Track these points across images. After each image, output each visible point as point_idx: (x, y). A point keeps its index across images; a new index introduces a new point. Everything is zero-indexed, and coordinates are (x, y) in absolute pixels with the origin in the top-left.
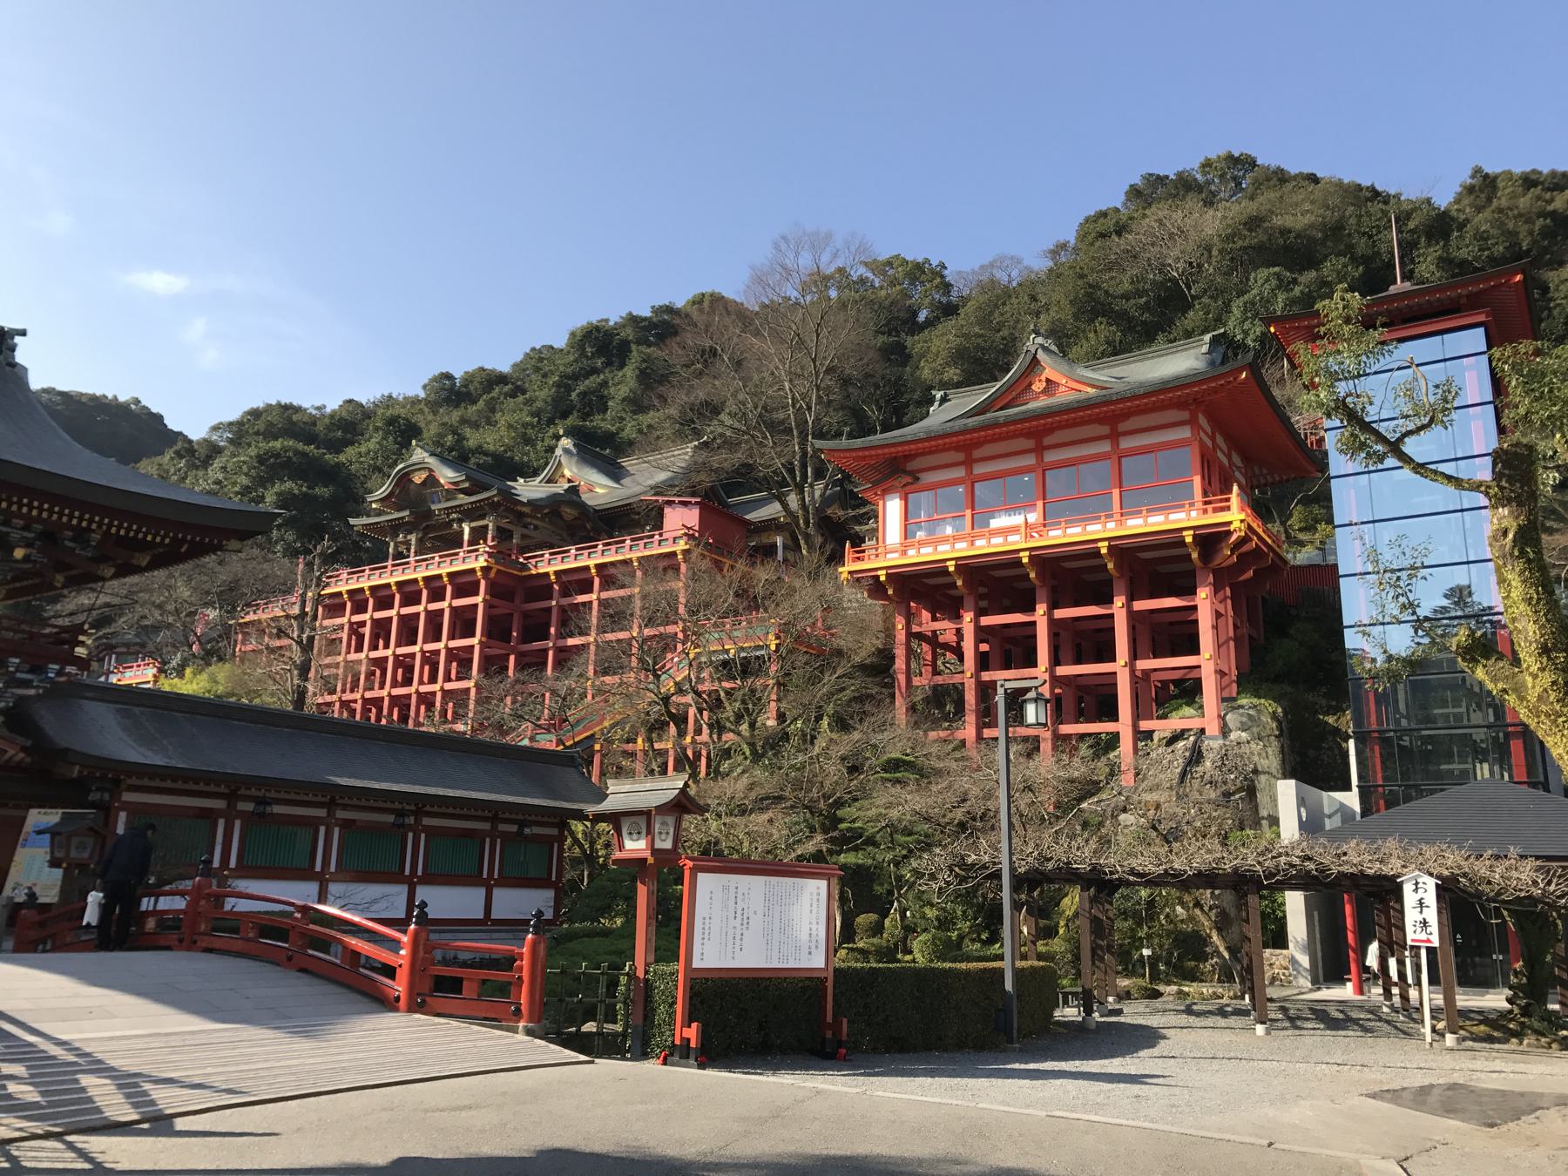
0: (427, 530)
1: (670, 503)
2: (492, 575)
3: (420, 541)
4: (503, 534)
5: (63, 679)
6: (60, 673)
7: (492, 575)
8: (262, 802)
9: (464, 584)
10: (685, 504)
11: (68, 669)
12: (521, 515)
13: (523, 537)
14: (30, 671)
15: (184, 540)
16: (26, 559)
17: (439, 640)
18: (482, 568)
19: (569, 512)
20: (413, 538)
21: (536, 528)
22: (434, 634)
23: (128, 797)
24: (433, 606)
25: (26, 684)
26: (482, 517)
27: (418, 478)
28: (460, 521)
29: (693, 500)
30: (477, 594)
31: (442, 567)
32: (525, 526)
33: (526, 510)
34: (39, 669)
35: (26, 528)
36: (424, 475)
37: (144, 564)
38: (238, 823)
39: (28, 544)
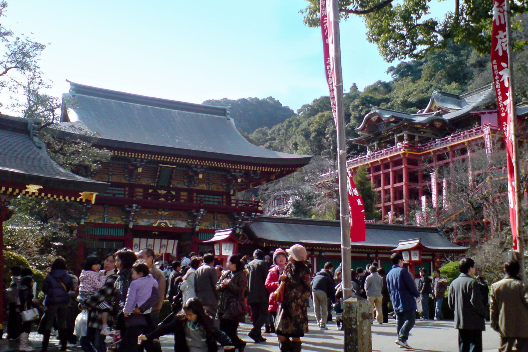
0: (380, 140)
1: (483, 113)
2: (407, 156)
3: (379, 145)
4: (411, 138)
6: (255, 215)
7: (407, 156)
8: (321, 251)
9: (396, 161)
10: (490, 113)
11: (258, 214)
12: (417, 129)
13: (419, 137)
14: (247, 216)
15: (284, 170)
16: (242, 181)
17: (389, 184)
18: (403, 154)
19: (438, 124)
20: (375, 144)
21: (424, 132)
22: (387, 182)
24: (386, 171)
25: (247, 219)
26: (401, 132)
27: (374, 118)
28: (393, 135)
29: (494, 111)
30: (402, 164)
31: (386, 155)
32: (420, 132)
33: (419, 126)
34: (250, 215)
35: (240, 172)
36: (376, 117)
37: (274, 178)
38: (315, 259)
39: (241, 177)
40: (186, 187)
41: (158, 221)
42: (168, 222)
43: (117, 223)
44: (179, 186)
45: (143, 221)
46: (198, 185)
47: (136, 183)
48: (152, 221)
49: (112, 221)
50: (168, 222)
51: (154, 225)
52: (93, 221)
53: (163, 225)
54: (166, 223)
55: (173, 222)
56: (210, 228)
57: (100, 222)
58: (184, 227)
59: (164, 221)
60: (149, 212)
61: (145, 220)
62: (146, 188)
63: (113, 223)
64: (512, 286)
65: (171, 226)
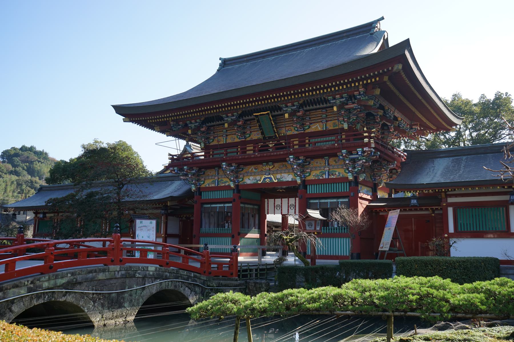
5: (366, 154)
6: (364, 152)
11: (365, 149)
23: (450, 200)
40: (296, 133)
41: (263, 177)
42: (272, 177)
43: (227, 184)
44: (289, 133)
45: (249, 179)
46: (309, 127)
47: (248, 139)
48: (258, 178)
49: (223, 183)
50: (272, 177)
51: (259, 182)
52: (207, 186)
53: (268, 181)
54: (270, 178)
55: (279, 176)
56: (321, 178)
57: (213, 185)
58: (290, 180)
59: (269, 176)
60: (256, 169)
61: (251, 178)
62: (255, 142)
63: (223, 185)
64: (231, 291)
65: (276, 181)
